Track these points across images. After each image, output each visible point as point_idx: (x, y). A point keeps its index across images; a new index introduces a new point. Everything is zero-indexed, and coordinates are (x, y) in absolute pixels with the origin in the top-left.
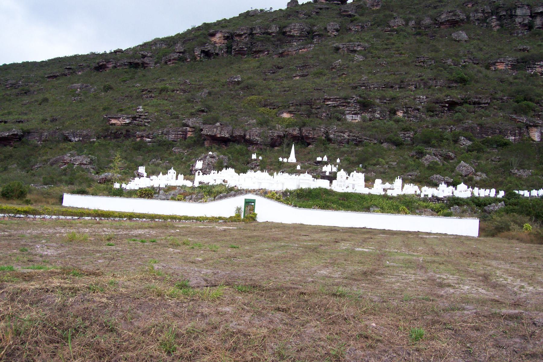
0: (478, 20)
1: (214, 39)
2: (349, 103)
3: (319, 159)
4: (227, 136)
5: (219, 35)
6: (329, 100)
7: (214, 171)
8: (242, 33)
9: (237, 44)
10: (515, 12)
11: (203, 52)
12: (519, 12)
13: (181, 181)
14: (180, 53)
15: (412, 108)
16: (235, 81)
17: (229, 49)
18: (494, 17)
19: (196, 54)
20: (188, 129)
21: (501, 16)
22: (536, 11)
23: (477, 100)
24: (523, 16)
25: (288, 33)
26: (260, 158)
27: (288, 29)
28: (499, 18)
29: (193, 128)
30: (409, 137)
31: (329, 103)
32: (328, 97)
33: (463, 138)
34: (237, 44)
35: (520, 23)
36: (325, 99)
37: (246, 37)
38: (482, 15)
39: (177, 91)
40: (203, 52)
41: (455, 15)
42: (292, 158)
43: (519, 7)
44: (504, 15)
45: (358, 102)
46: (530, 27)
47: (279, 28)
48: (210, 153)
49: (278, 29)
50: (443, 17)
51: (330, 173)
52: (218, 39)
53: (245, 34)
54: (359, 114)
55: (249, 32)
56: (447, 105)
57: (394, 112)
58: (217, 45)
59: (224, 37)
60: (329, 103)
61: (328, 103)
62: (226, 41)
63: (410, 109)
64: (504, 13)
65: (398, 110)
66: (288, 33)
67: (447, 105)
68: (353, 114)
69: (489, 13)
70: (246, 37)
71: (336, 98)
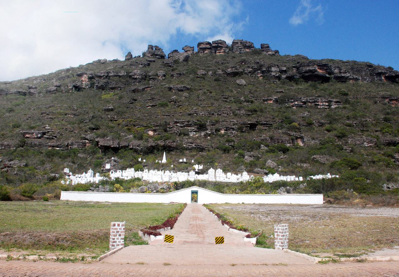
0: (250, 72)
3: (181, 161)
7: (119, 171)
8: (102, 75)
12: (273, 69)
13: (98, 178)
16: (110, 109)
17: (92, 85)
18: (259, 71)
20: (87, 141)
22: (282, 69)
23: (265, 122)
24: (275, 71)
25: (133, 77)
26: (144, 161)
28: (263, 72)
29: (91, 140)
30: (231, 145)
35: (274, 76)
39: (69, 114)
41: (237, 69)
42: (164, 160)
43: (273, 66)
44: (265, 71)
46: (279, 78)
47: (126, 73)
49: (126, 74)
50: (229, 70)
51: (198, 170)
52: (85, 78)
53: (104, 76)
55: (106, 75)
57: (218, 130)
59: (88, 77)
60: (178, 124)
64: (265, 69)
68: (194, 131)
69: (256, 68)
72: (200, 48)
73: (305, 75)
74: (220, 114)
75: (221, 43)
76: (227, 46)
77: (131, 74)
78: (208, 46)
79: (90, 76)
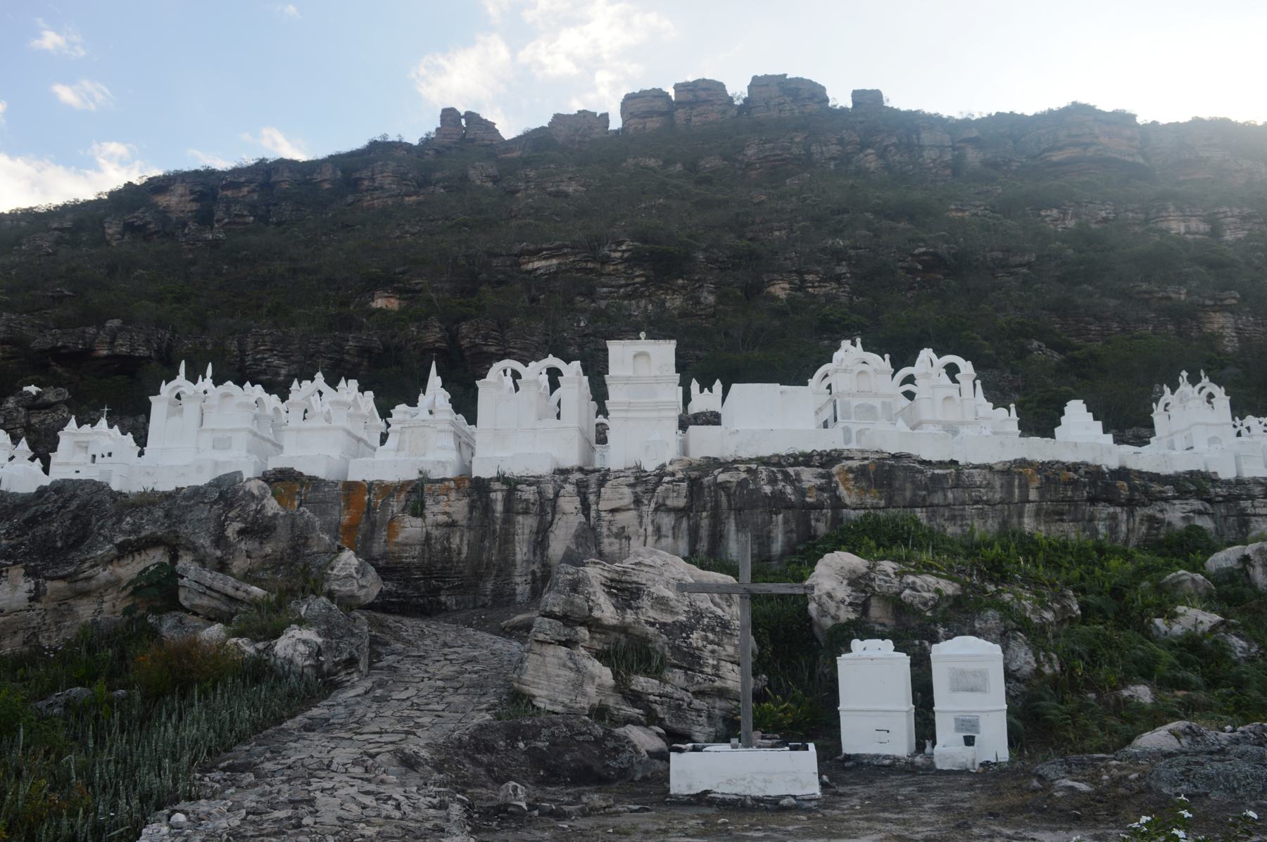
1: (162, 200)
2: (606, 260)
4: (142, 351)
5: (180, 189)
6: (535, 253)
8: (242, 179)
9: (228, 208)
10: (918, 139)
11: (129, 227)
14: (62, 230)
15: (817, 273)
16: (206, 240)
17: (205, 218)
18: (870, 151)
19: (110, 231)
21: (887, 147)
27: (366, 173)
31: (537, 264)
32: (531, 247)
33: (1036, 344)
34: (228, 208)
35: (934, 161)
36: (522, 254)
37: (253, 191)
38: (839, 148)
40: (129, 227)
45: (635, 259)
47: (343, 171)
48: (33, 389)
49: (339, 174)
53: (249, 182)
54: (642, 296)
56: (920, 267)
57: (754, 291)
58: (173, 217)
59: (192, 193)
60: (537, 264)
61: (530, 266)
62: (194, 206)
63: (809, 277)
64: (894, 140)
65: (771, 283)
66: (366, 183)
67: (920, 267)
70: (253, 191)
71: (559, 248)
72: (633, 115)
73: (1054, 159)
74: (750, 235)
75: (704, 89)
76: (731, 99)
77: (357, 175)
78: (659, 105)
79: (200, 188)
